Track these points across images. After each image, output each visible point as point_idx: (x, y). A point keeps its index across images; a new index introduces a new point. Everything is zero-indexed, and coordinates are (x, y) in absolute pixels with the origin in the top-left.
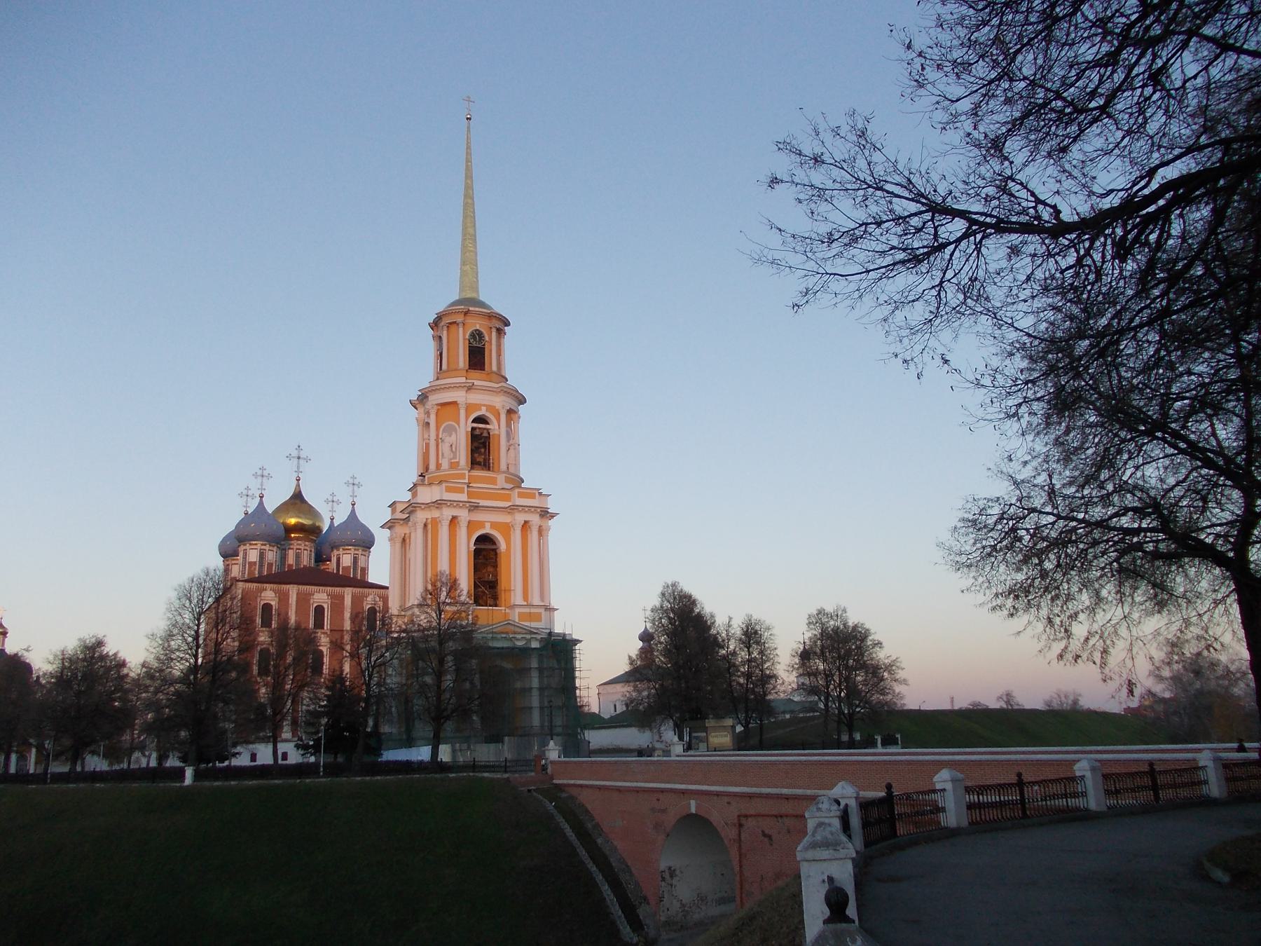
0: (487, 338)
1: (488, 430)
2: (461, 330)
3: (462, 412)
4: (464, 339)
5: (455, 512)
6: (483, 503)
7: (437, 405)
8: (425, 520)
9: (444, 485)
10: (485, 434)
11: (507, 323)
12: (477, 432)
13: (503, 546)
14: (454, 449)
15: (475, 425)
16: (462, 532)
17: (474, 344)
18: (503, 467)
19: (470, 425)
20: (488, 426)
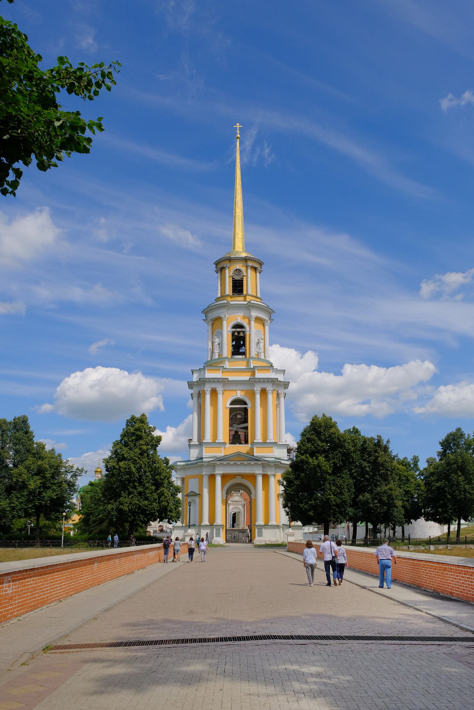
0: (245, 274)
1: (243, 332)
2: (227, 271)
3: (225, 323)
4: (230, 277)
5: (213, 386)
6: (230, 378)
7: (211, 320)
8: (198, 392)
9: (206, 369)
10: (242, 335)
11: (261, 264)
12: (236, 334)
13: (249, 406)
14: (220, 346)
15: (234, 330)
16: (220, 397)
17: (237, 278)
18: (253, 354)
19: (230, 329)
20: (243, 330)
